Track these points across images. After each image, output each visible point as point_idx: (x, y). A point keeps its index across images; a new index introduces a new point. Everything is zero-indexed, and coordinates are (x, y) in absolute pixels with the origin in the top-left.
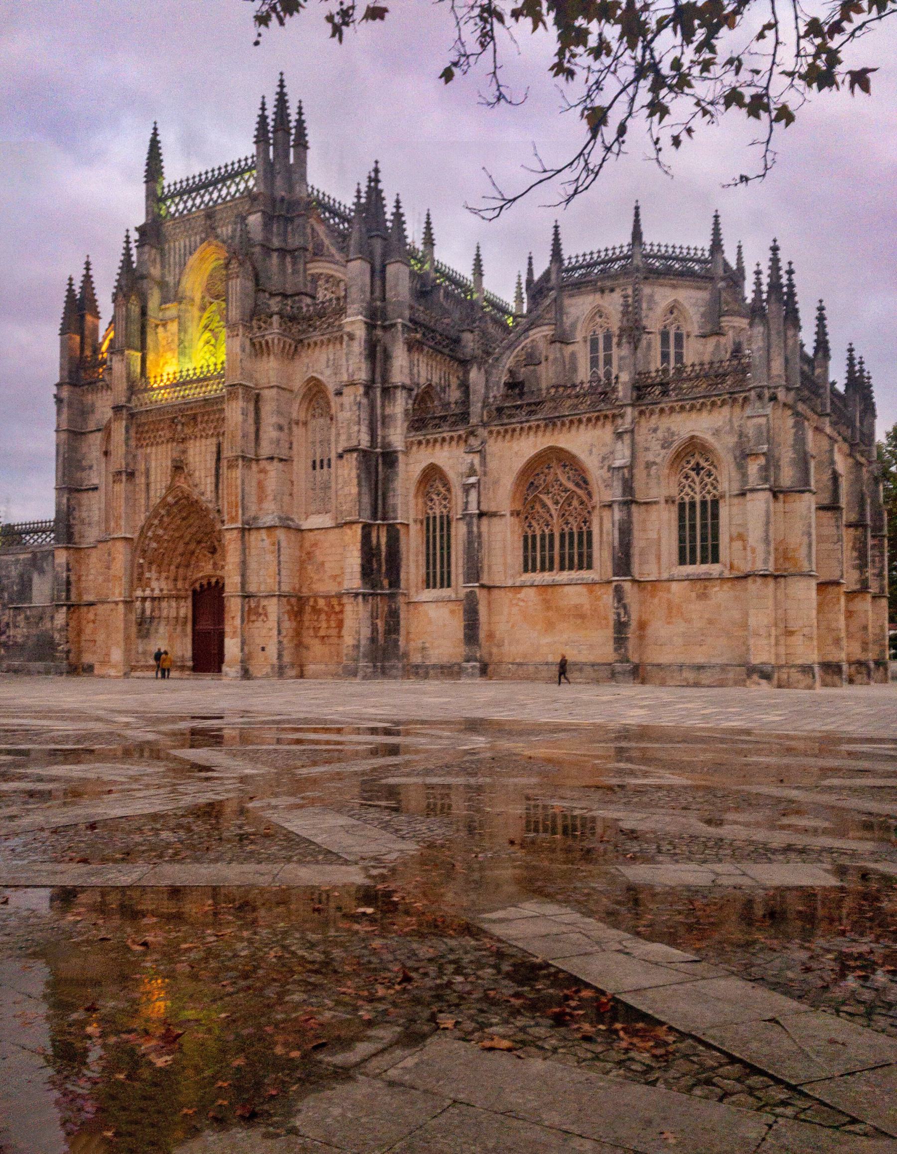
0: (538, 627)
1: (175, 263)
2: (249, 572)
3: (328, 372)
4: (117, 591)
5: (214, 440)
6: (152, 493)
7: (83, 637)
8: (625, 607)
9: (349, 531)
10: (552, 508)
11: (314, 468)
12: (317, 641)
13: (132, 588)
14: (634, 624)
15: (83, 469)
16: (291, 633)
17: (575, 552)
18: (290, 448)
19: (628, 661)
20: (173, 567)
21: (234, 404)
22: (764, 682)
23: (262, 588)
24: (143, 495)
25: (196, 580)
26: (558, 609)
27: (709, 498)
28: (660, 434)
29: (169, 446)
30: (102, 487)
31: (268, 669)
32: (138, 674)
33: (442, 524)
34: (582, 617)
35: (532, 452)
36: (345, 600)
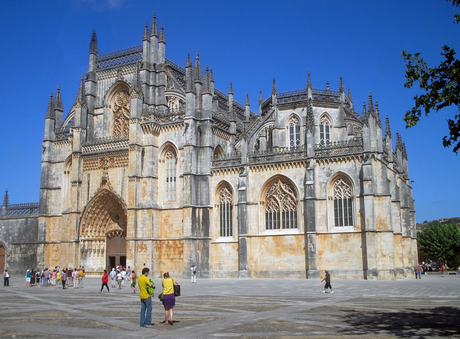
0: (273, 254)
1: (102, 89)
2: (138, 229)
3: (175, 139)
4: (72, 237)
6: (90, 192)
7: (50, 259)
8: (313, 245)
10: (279, 200)
11: (168, 181)
12: (169, 261)
14: (317, 252)
15: (54, 179)
16: (157, 257)
18: (157, 172)
22: (374, 277)
23: (145, 236)
24: (86, 192)
26: (283, 246)
30: (63, 188)
34: (293, 249)
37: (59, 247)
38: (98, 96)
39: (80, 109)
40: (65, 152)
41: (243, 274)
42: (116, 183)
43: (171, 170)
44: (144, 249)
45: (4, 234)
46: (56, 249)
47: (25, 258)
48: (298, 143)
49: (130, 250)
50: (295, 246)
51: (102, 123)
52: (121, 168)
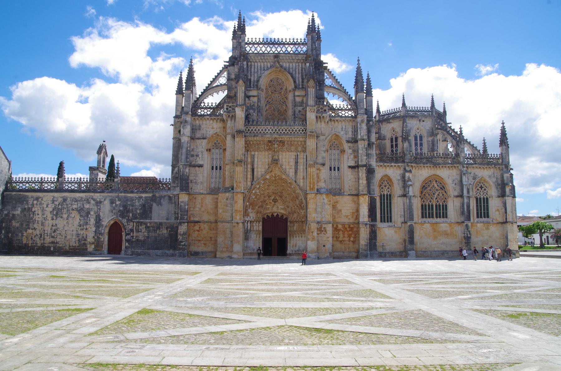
1: (254, 72)
3: (342, 133)
4: (238, 218)
5: (295, 154)
6: (255, 173)
7: (190, 238)
8: (469, 231)
12: (338, 243)
13: (244, 217)
15: (193, 156)
17: (441, 211)
21: (311, 140)
23: (324, 220)
27: (485, 197)
28: (472, 175)
29: (267, 153)
30: (205, 166)
31: (328, 255)
32: (247, 257)
34: (447, 235)
36: (361, 226)
38: (249, 78)
39: (243, 88)
42: (287, 167)
43: (335, 160)
45: (120, 211)
46: (198, 229)
48: (421, 149)
50: (449, 232)
51: (256, 106)
52: (295, 154)
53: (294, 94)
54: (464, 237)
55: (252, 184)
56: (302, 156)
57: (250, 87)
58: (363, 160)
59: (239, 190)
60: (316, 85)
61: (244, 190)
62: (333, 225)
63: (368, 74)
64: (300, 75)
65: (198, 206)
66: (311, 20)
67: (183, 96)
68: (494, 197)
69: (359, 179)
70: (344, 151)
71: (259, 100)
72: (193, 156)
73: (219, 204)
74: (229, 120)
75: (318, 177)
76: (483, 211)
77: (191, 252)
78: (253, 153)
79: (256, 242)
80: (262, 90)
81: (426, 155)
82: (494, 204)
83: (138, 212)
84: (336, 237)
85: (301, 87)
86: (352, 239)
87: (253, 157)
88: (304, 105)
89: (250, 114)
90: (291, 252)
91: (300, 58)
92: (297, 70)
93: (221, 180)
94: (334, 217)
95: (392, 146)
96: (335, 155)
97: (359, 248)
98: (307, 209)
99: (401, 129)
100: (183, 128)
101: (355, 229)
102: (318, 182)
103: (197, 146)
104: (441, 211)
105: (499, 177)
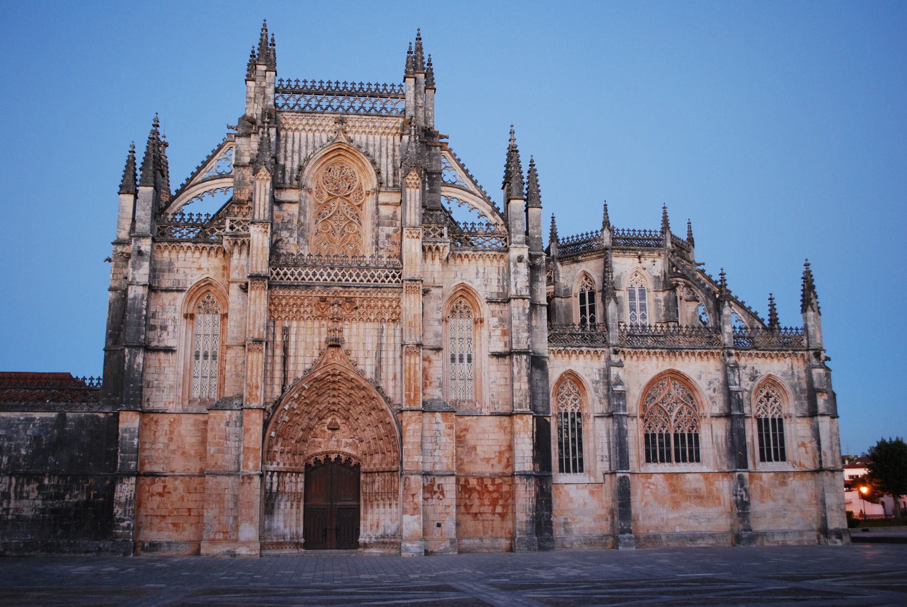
0: (666, 506)
1: (293, 151)
4: (251, 465)
6: (291, 367)
8: (746, 490)
9: (519, 421)
15: (153, 328)
17: (687, 448)
19: (750, 530)
20: (293, 442)
21: (412, 297)
22: (838, 541)
23: (438, 467)
24: (278, 367)
25: (312, 456)
26: (682, 492)
27: (777, 417)
29: (316, 324)
30: (181, 351)
31: (448, 544)
32: (268, 552)
33: (573, 420)
35: (656, 372)
36: (517, 480)
37: (170, 486)
39: (268, 184)
40: (187, 271)
41: (627, 541)
42: (361, 354)
44: (438, 494)
46: (160, 490)
47: (55, 511)
48: (644, 317)
49: (413, 495)
50: (704, 490)
51: (295, 222)
53: (377, 198)
54: (736, 502)
55: (283, 391)
56: (392, 332)
57: (284, 183)
58: (522, 341)
59: (254, 404)
60: (424, 182)
61: (266, 403)
62: (458, 481)
63: (532, 161)
64: (390, 159)
65: (163, 439)
66: (413, 46)
67: (136, 198)
68: (793, 416)
69: (512, 379)
70: (482, 321)
71: (302, 212)
72: (153, 328)
73: (210, 435)
74: (236, 250)
75: (426, 376)
76: (773, 445)
77: (143, 543)
78: (286, 324)
79: (289, 521)
80: (310, 191)
81: (653, 329)
82: (796, 431)
83: (23, 452)
84: (465, 505)
85: (391, 184)
86: (499, 509)
87: (286, 331)
88: (398, 223)
89: (281, 240)
90: (367, 540)
91: (391, 125)
92: (384, 149)
93: (215, 382)
94: (459, 461)
95: (583, 311)
96: (461, 328)
97: (514, 528)
98: (402, 445)
99: (601, 274)
100: (134, 268)
101: (505, 488)
102: (425, 386)
103: (163, 307)
104: (687, 448)
105: (803, 375)
